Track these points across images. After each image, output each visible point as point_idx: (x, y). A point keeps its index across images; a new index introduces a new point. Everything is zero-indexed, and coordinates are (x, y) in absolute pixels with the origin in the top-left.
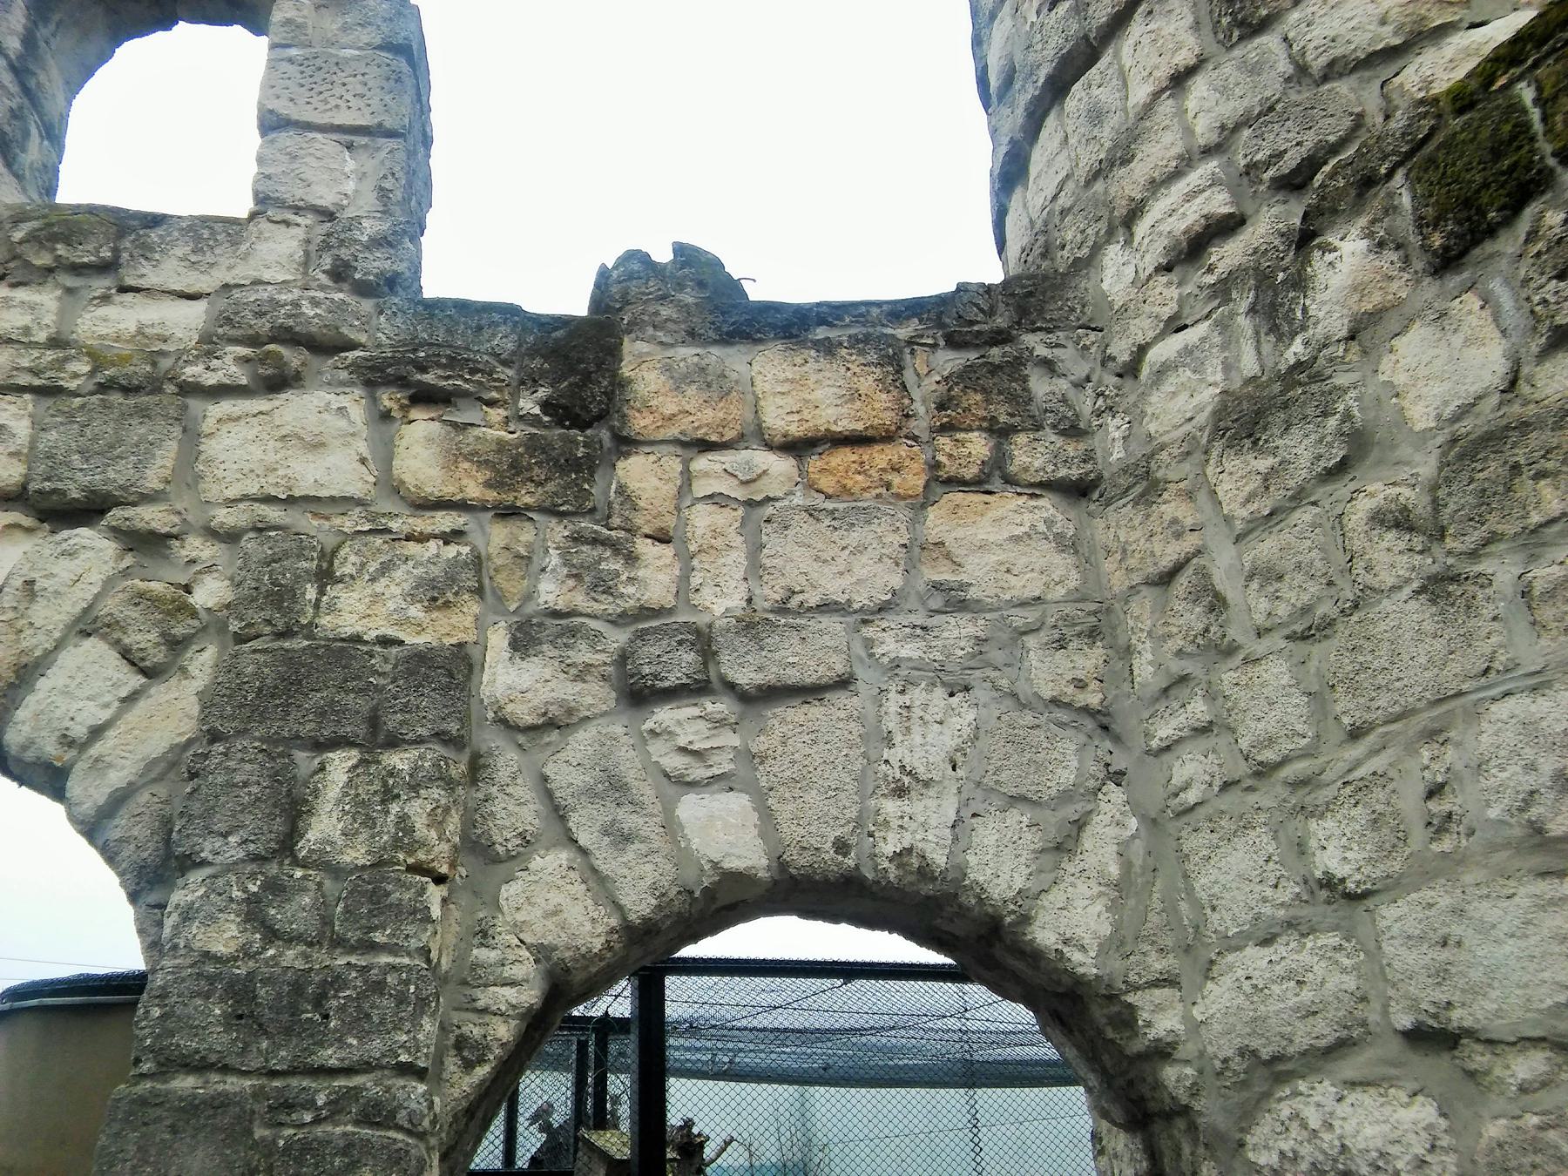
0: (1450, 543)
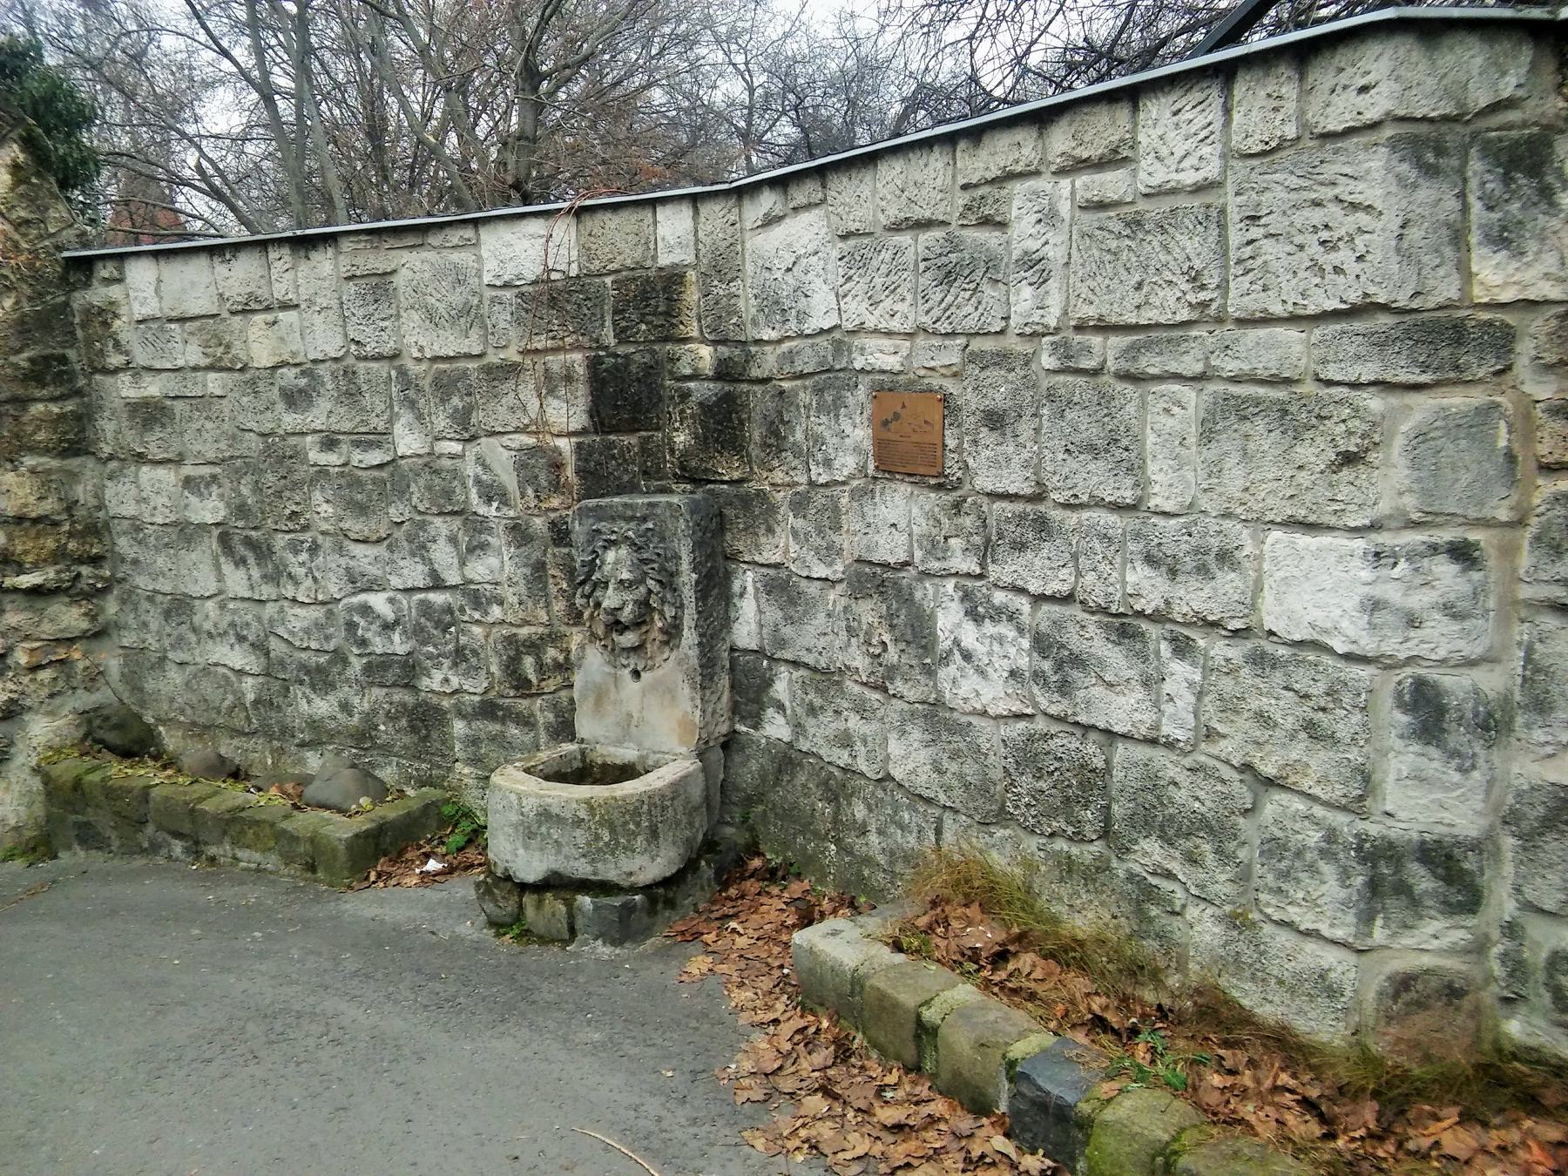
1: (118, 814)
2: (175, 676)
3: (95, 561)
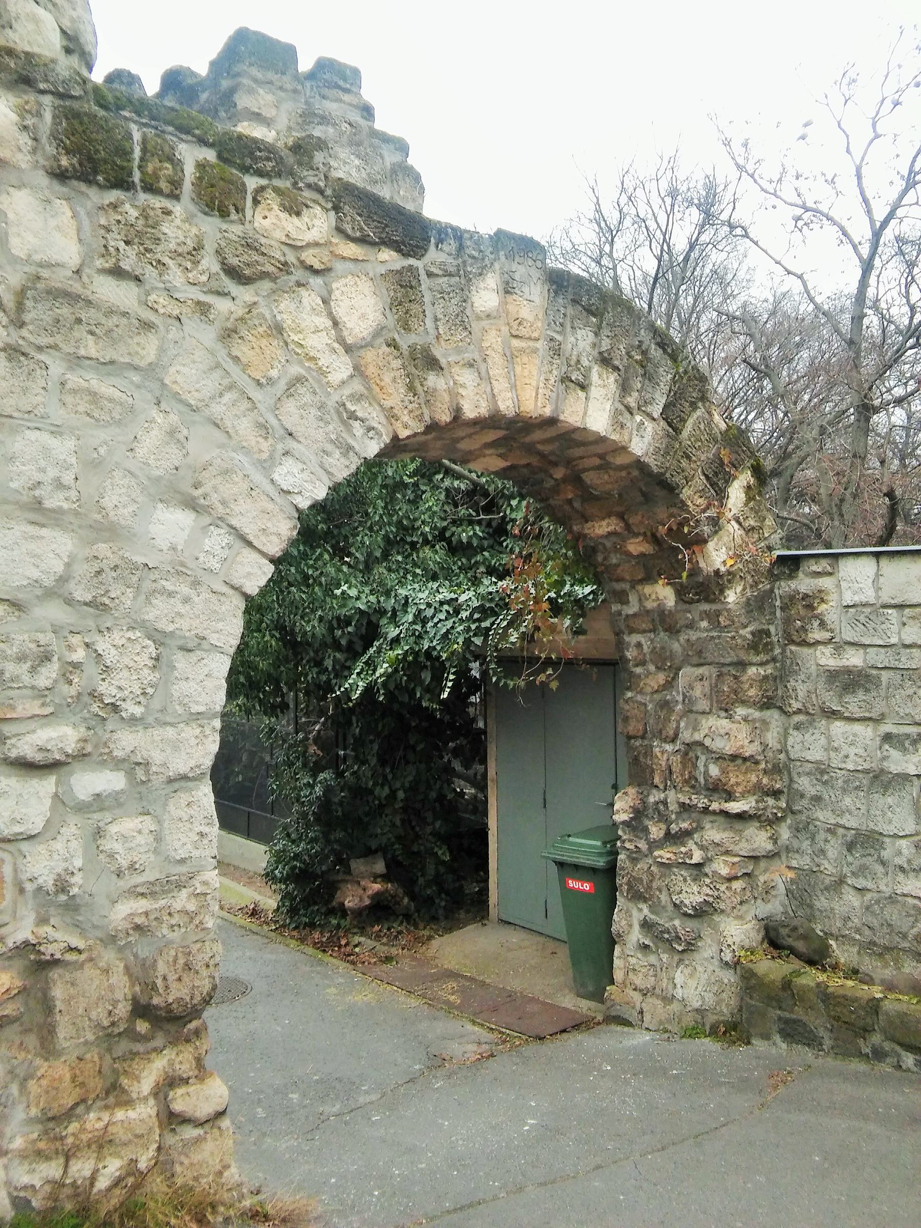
0: (24, 332)
1: (837, 1019)
2: (851, 899)
3: (776, 794)
